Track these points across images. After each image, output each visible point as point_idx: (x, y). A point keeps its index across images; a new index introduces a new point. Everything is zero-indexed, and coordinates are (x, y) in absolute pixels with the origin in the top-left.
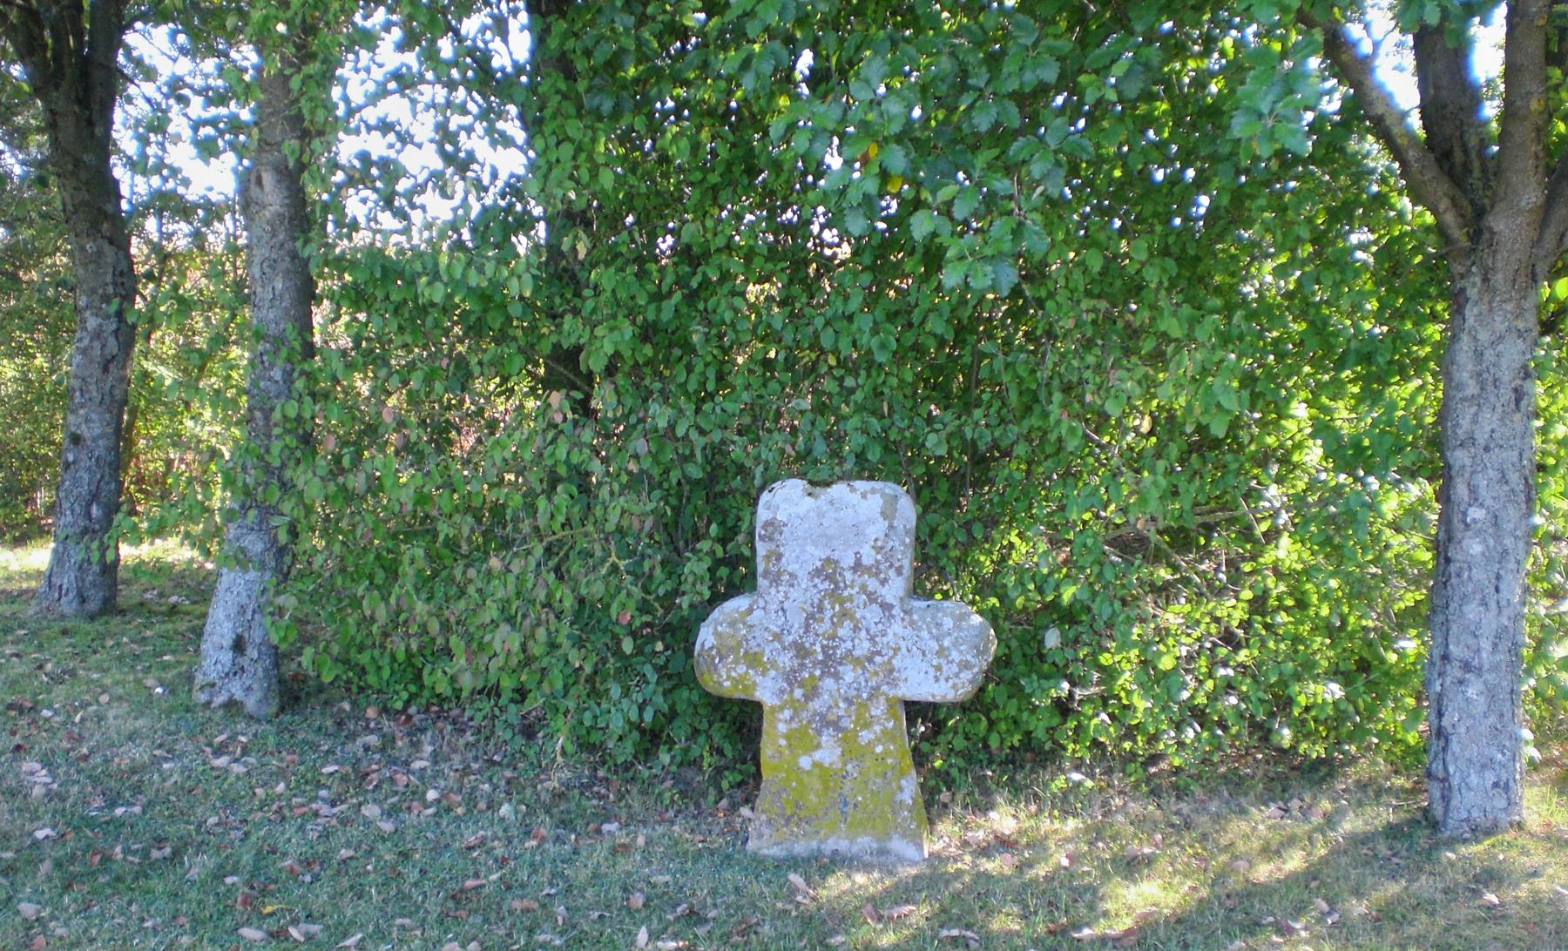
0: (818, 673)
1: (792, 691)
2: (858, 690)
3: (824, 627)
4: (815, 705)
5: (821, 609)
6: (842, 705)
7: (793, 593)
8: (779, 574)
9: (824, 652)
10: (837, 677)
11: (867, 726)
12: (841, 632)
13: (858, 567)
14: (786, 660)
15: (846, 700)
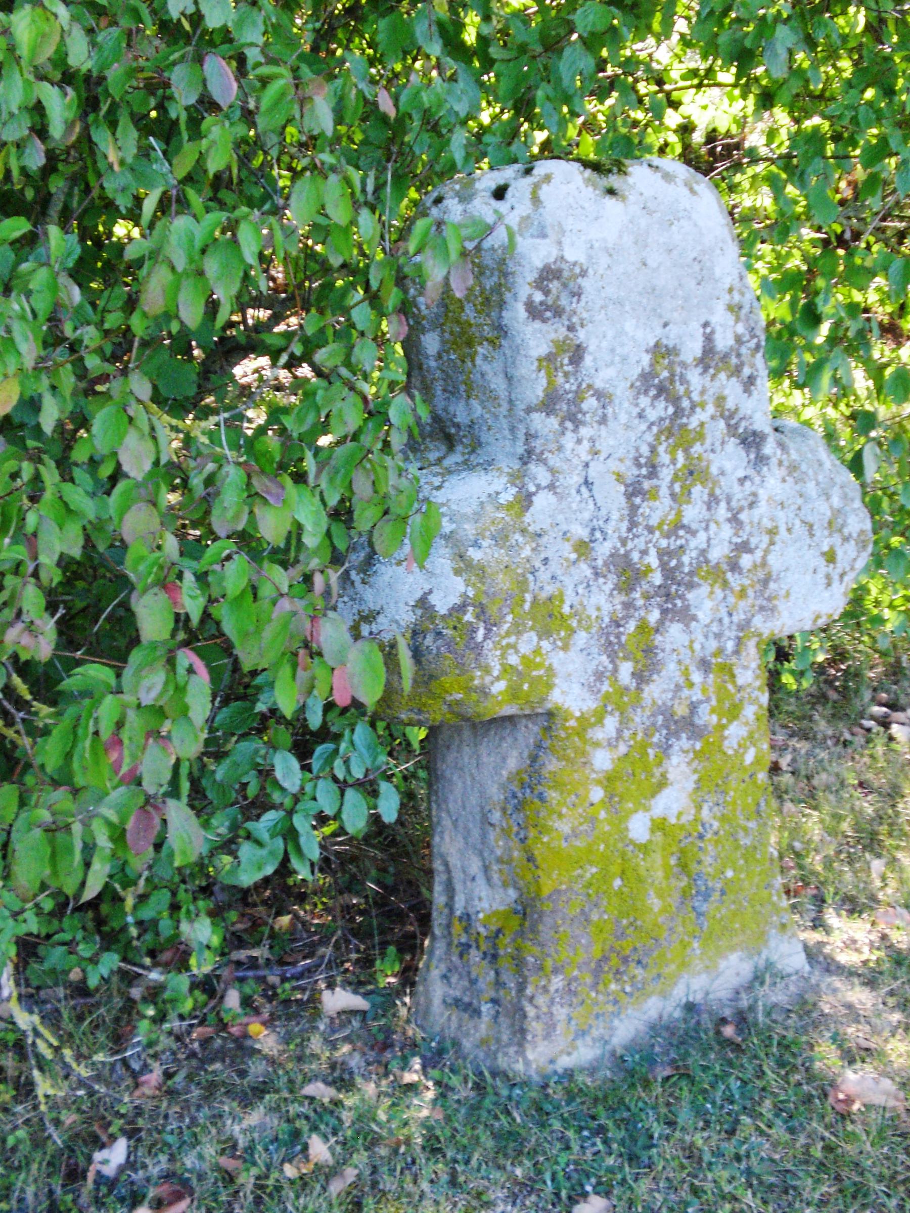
0: (654, 616)
2: (718, 636)
3: (657, 510)
4: (656, 691)
5: (653, 470)
7: (608, 440)
8: (579, 396)
9: (663, 566)
10: (686, 616)
12: (692, 513)
13: (709, 358)
14: (602, 601)
15: (705, 665)
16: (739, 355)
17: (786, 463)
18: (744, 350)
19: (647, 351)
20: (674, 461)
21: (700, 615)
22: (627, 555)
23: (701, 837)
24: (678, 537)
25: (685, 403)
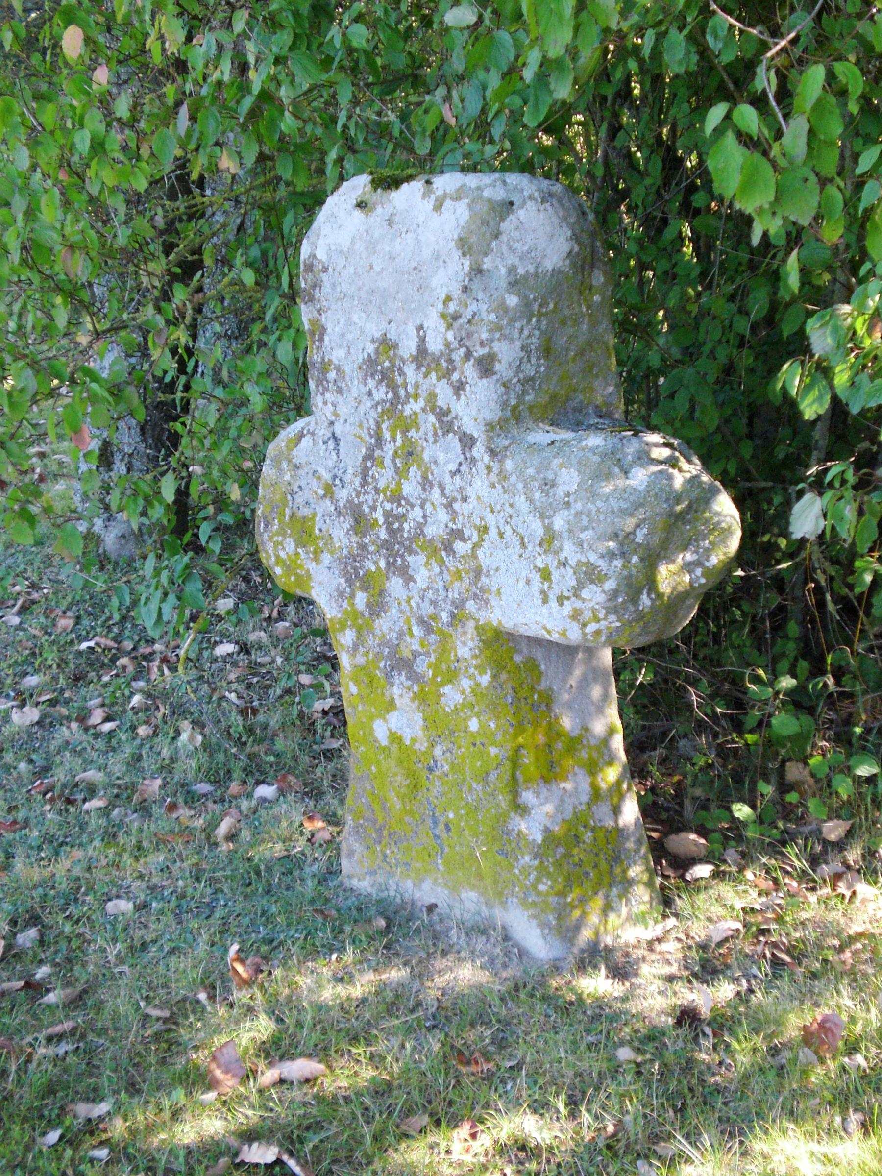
1: (353, 596)
2: (434, 603)
6: (416, 630)
11: (451, 677)
13: (422, 355)
14: (341, 534)
16: (450, 361)
17: (495, 470)
18: (454, 356)
19: (373, 341)
20: (394, 440)
21: (418, 578)
22: (360, 504)
23: (430, 770)
24: (399, 505)
25: (402, 393)
